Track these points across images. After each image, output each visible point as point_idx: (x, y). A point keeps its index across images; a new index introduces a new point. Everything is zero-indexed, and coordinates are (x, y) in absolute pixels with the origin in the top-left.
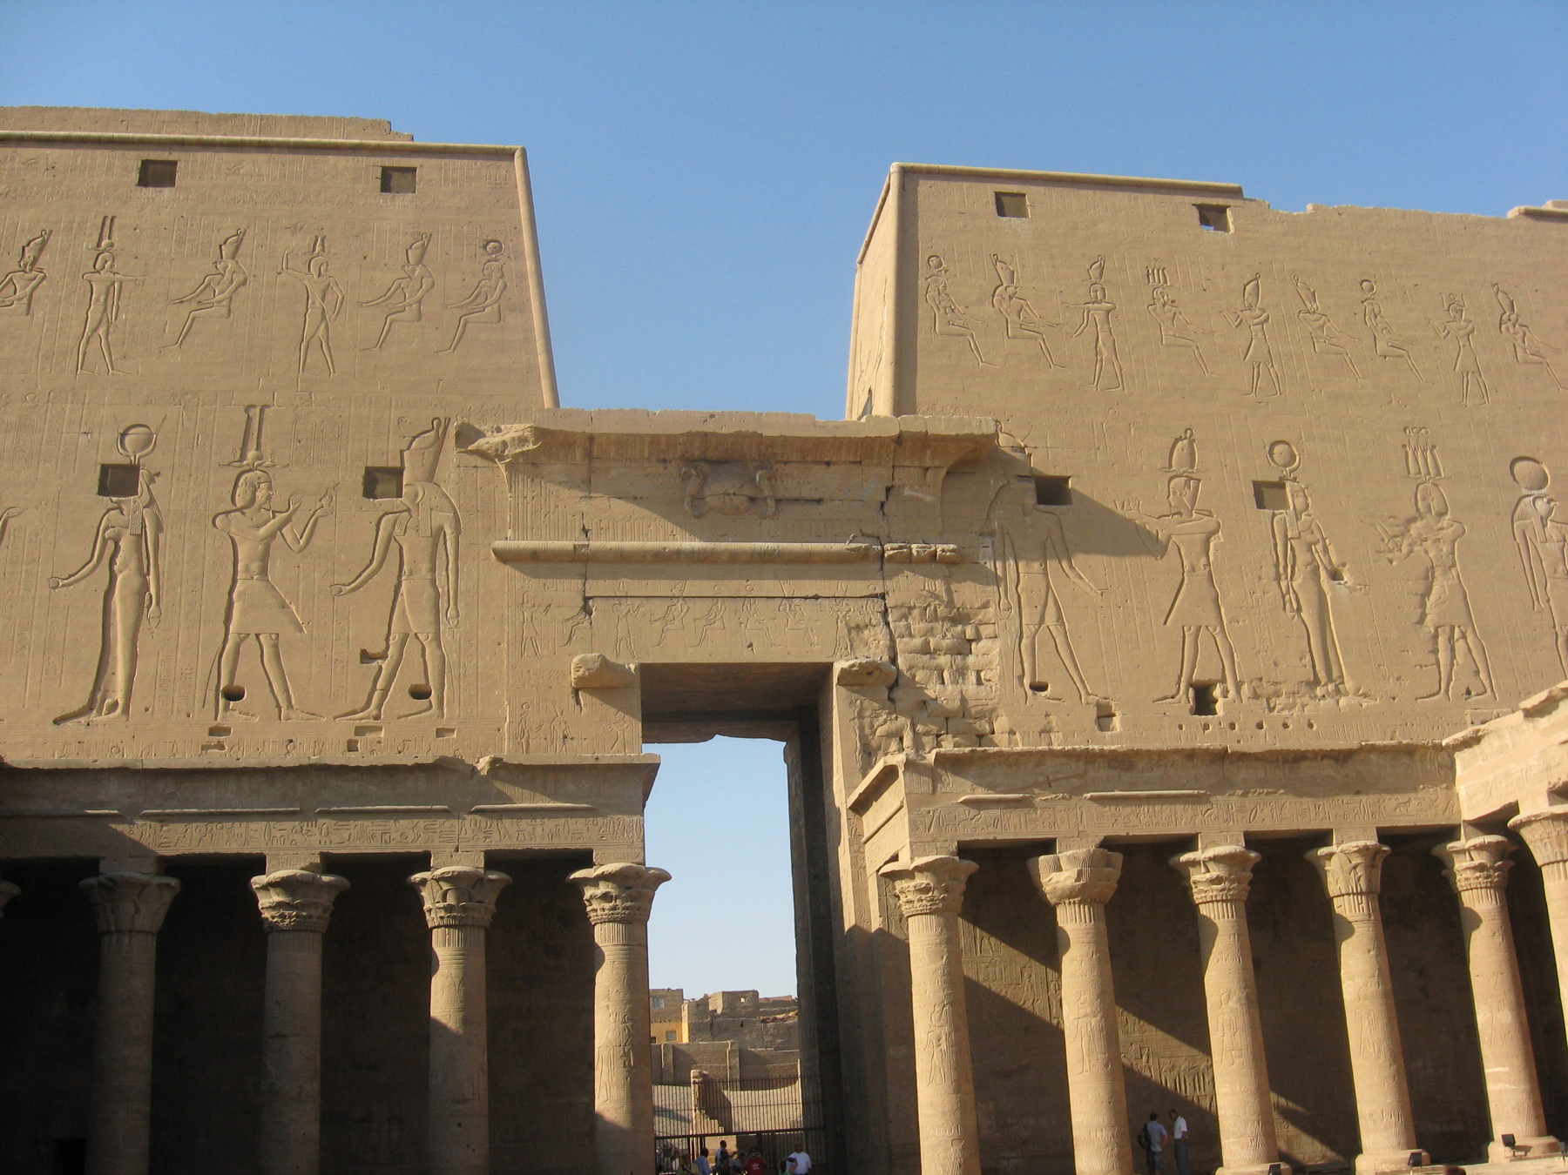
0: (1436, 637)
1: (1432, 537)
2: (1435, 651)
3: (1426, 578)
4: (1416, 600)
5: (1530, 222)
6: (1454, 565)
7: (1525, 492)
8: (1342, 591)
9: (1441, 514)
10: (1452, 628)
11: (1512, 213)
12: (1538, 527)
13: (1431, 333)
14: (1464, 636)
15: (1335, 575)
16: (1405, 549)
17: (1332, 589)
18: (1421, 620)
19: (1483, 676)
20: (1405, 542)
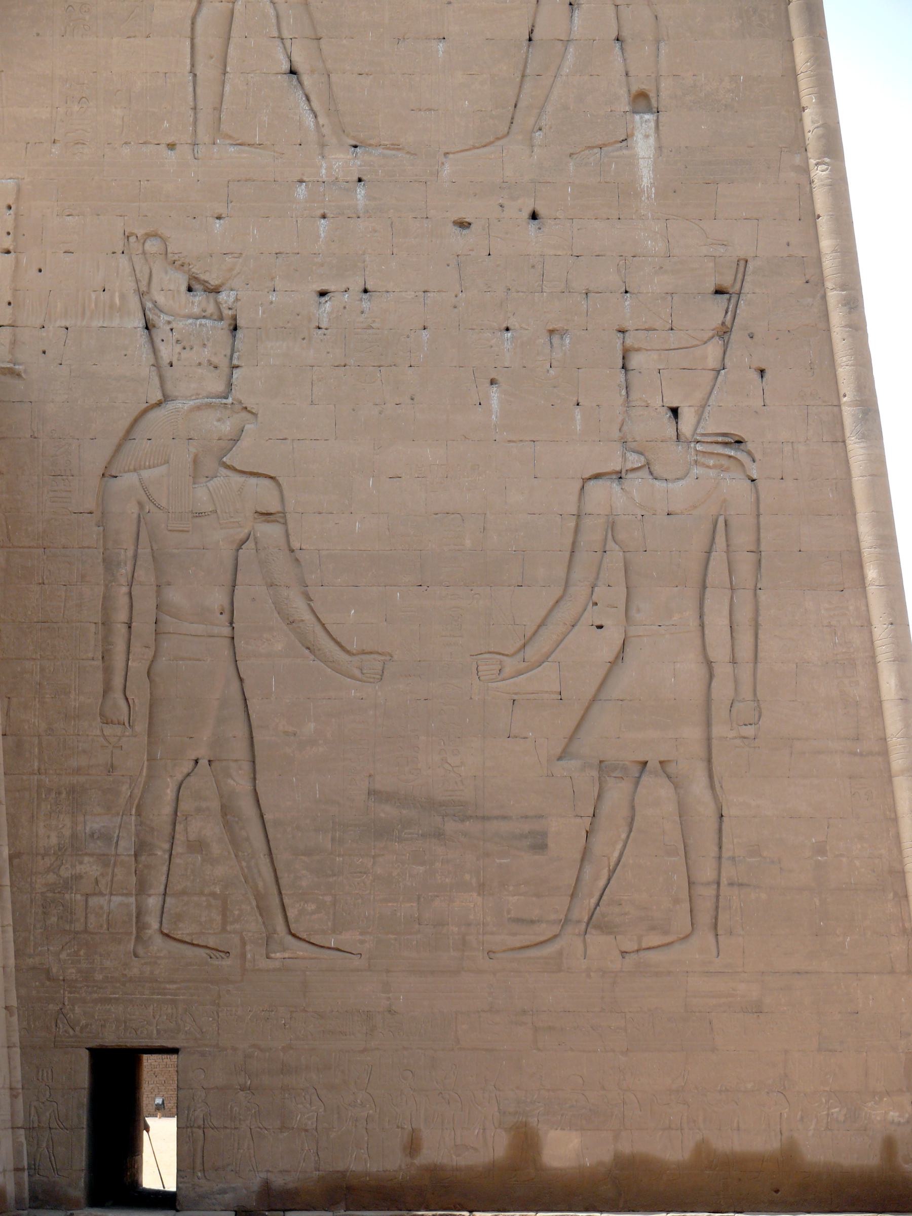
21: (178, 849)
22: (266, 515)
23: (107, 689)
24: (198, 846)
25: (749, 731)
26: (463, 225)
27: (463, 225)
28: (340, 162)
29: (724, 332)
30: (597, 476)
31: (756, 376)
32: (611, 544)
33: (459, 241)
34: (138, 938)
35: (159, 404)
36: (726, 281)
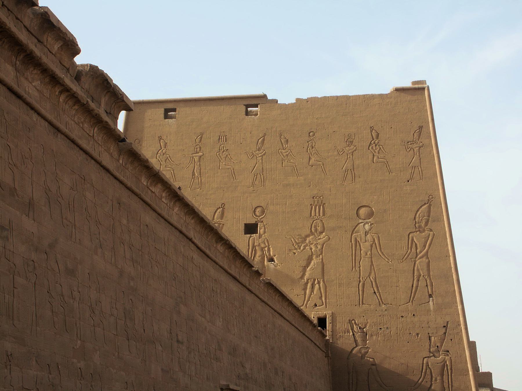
0: (307, 283)
2: (305, 289)
5: (398, 93)
6: (321, 254)
7: (360, 221)
8: (271, 265)
9: (321, 233)
10: (314, 280)
12: (363, 236)
13: (336, 153)
14: (319, 283)
16: (302, 248)
20: (303, 245)
22: (373, 365)
26: (402, 317)
27: (402, 317)
29: (445, 333)
30: (426, 357)
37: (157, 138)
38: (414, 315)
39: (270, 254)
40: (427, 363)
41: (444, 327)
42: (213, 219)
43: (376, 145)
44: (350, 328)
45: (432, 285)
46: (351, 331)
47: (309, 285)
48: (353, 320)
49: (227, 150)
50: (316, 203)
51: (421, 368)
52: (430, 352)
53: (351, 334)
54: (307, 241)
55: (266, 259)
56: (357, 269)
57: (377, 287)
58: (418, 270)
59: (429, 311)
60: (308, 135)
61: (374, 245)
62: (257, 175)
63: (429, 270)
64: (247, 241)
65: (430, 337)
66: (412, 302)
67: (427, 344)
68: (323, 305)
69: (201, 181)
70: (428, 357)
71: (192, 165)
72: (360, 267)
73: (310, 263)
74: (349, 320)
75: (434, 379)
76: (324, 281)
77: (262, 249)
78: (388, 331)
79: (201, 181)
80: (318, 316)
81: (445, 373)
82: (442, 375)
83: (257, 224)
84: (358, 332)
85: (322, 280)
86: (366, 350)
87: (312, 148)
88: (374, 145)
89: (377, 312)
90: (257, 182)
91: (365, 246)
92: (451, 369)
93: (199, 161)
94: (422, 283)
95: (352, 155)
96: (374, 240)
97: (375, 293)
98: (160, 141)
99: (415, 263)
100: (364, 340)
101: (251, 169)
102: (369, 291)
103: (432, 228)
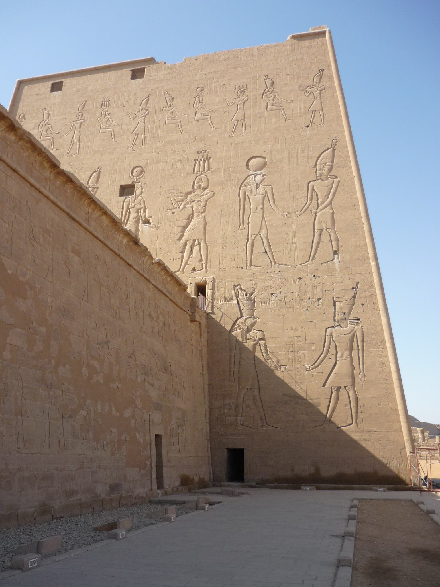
0: (185, 245)
1: (197, 199)
2: (183, 252)
3: (188, 219)
4: (180, 229)
6: (204, 211)
7: (251, 173)
10: (194, 241)
11: (289, 38)
12: (254, 189)
13: (225, 105)
14: (199, 244)
15: (147, 222)
16: (181, 207)
17: (142, 228)
18: (180, 239)
19: (204, 262)
20: (183, 203)
21: (244, 407)
23: (230, 375)
24: (248, 406)
25: (363, 379)
26: (300, 279)
27: (300, 279)
28: (276, 268)
29: (354, 297)
30: (329, 328)
31: (361, 305)
32: (332, 341)
33: (300, 282)
34: (236, 425)
35: (240, 318)
36: (355, 286)
37: (41, 111)
38: (314, 276)
39: (145, 216)
40: (331, 334)
41: (353, 289)
42: (88, 183)
43: (270, 94)
44: (234, 295)
45: (337, 239)
46: (235, 298)
47: (188, 247)
48: (238, 285)
49: (109, 114)
50: (200, 157)
51: (323, 341)
52: (334, 320)
53: (235, 302)
54: (188, 199)
55: (140, 221)
56: (246, 226)
57: (269, 246)
58: (320, 223)
59: (334, 270)
60: (195, 90)
61: (266, 197)
62: (138, 135)
63: (333, 224)
64: (122, 203)
65: (335, 302)
66: (312, 260)
67: (332, 311)
68: (203, 269)
69: (80, 146)
70: (333, 327)
71: (73, 132)
72: (248, 224)
73: (191, 222)
74: (234, 286)
75: (339, 354)
76: (205, 242)
77: (138, 211)
78: (282, 296)
79: (80, 146)
80: (196, 281)
81: (355, 346)
82: (351, 349)
83: (134, 185)
84: (244, 299)
85: (203, 241)
86: (253, 321)
87: (199, 103)
88: (268, 93)
89: (268, 275)
90: (137, 142)
91: (255, 199)
92: (363, 342)
93: (80, 127)
94: (325, 238)
95: (244, 105)
96: (266, 193)
97: (266, 252)
98: (43, 112)
99: (316, 216)
100: (252, 309)
101: (132, 129)
102: (259, 249)
103: (337, 175)
